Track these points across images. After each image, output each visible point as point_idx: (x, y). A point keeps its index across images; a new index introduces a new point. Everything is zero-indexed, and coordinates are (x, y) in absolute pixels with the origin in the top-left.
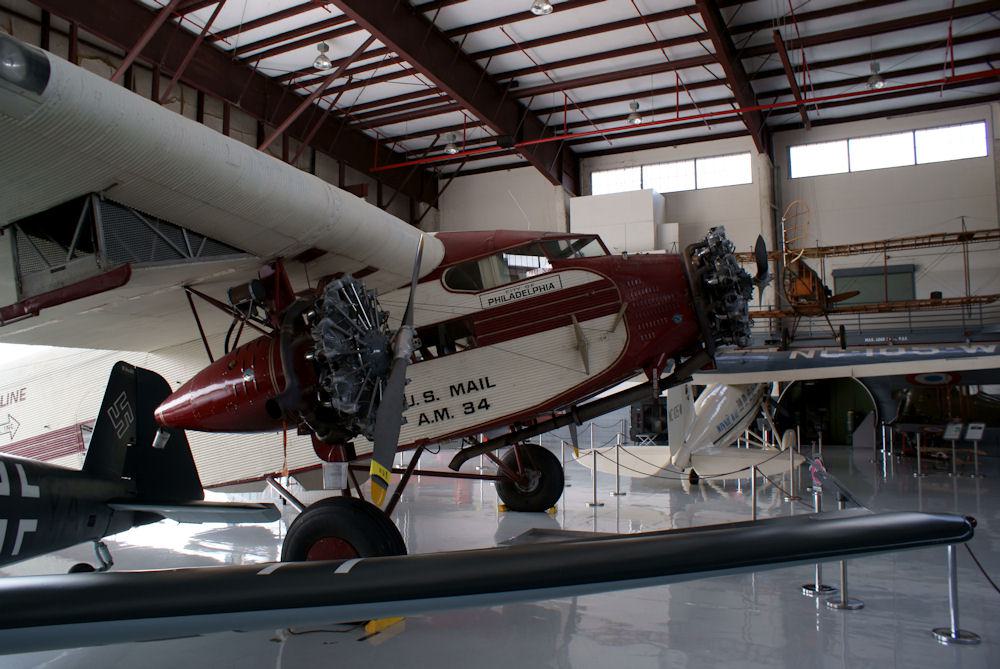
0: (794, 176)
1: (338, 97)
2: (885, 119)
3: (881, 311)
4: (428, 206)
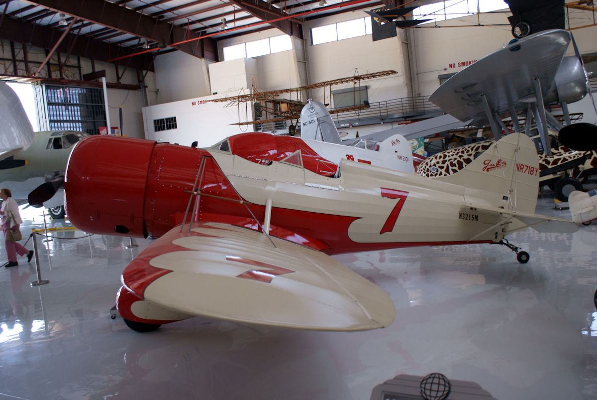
0: (314, 43)
1: (80, 31)
2: (351, 12)
3: (343, 111)
4: (146, 71)
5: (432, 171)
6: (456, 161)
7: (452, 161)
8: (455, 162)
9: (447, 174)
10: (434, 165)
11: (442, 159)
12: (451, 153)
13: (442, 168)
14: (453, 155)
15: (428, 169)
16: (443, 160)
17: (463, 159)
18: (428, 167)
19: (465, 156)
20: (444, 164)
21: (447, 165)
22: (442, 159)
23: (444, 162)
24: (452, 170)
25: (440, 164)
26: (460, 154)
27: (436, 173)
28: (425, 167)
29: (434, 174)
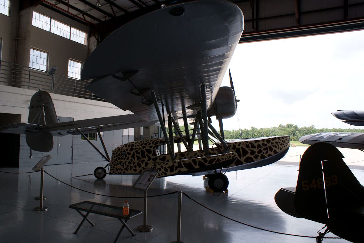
5: (122, 155)
6: (140, 150)
7: (138, 149)
8: (139, 151)
9: (133, 160)
10: (124, 151)
11: (130, 147)
12: (137, 144)
13: (129, 154)
14: (138, 145)
15: (119, 154)
16: (131, 148)
17: (146, 149)
18: (119, 152)
19: (148, 148)
20: (131, 151)
21: (134, 152)
22: (130, 147)
23: (131, 150)
24: (137, 156)
25: (129, 151)
26: (144, 145)
27: (125, 157)
28: (118, 152)
29: (123, 158)
